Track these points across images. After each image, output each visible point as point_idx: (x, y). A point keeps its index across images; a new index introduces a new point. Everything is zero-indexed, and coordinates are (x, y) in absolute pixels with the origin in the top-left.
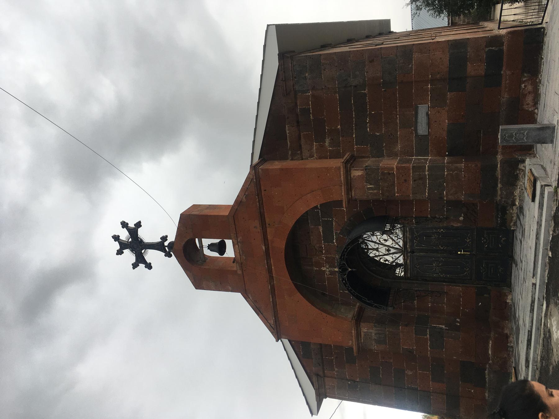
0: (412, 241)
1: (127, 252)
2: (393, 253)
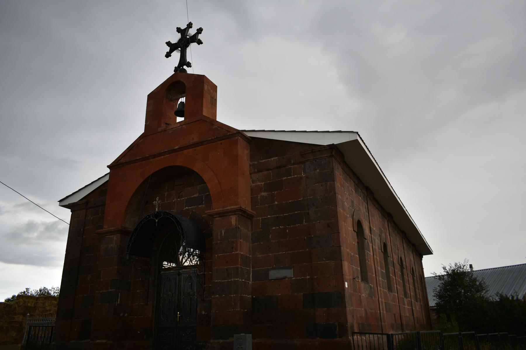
1: (179, 36)
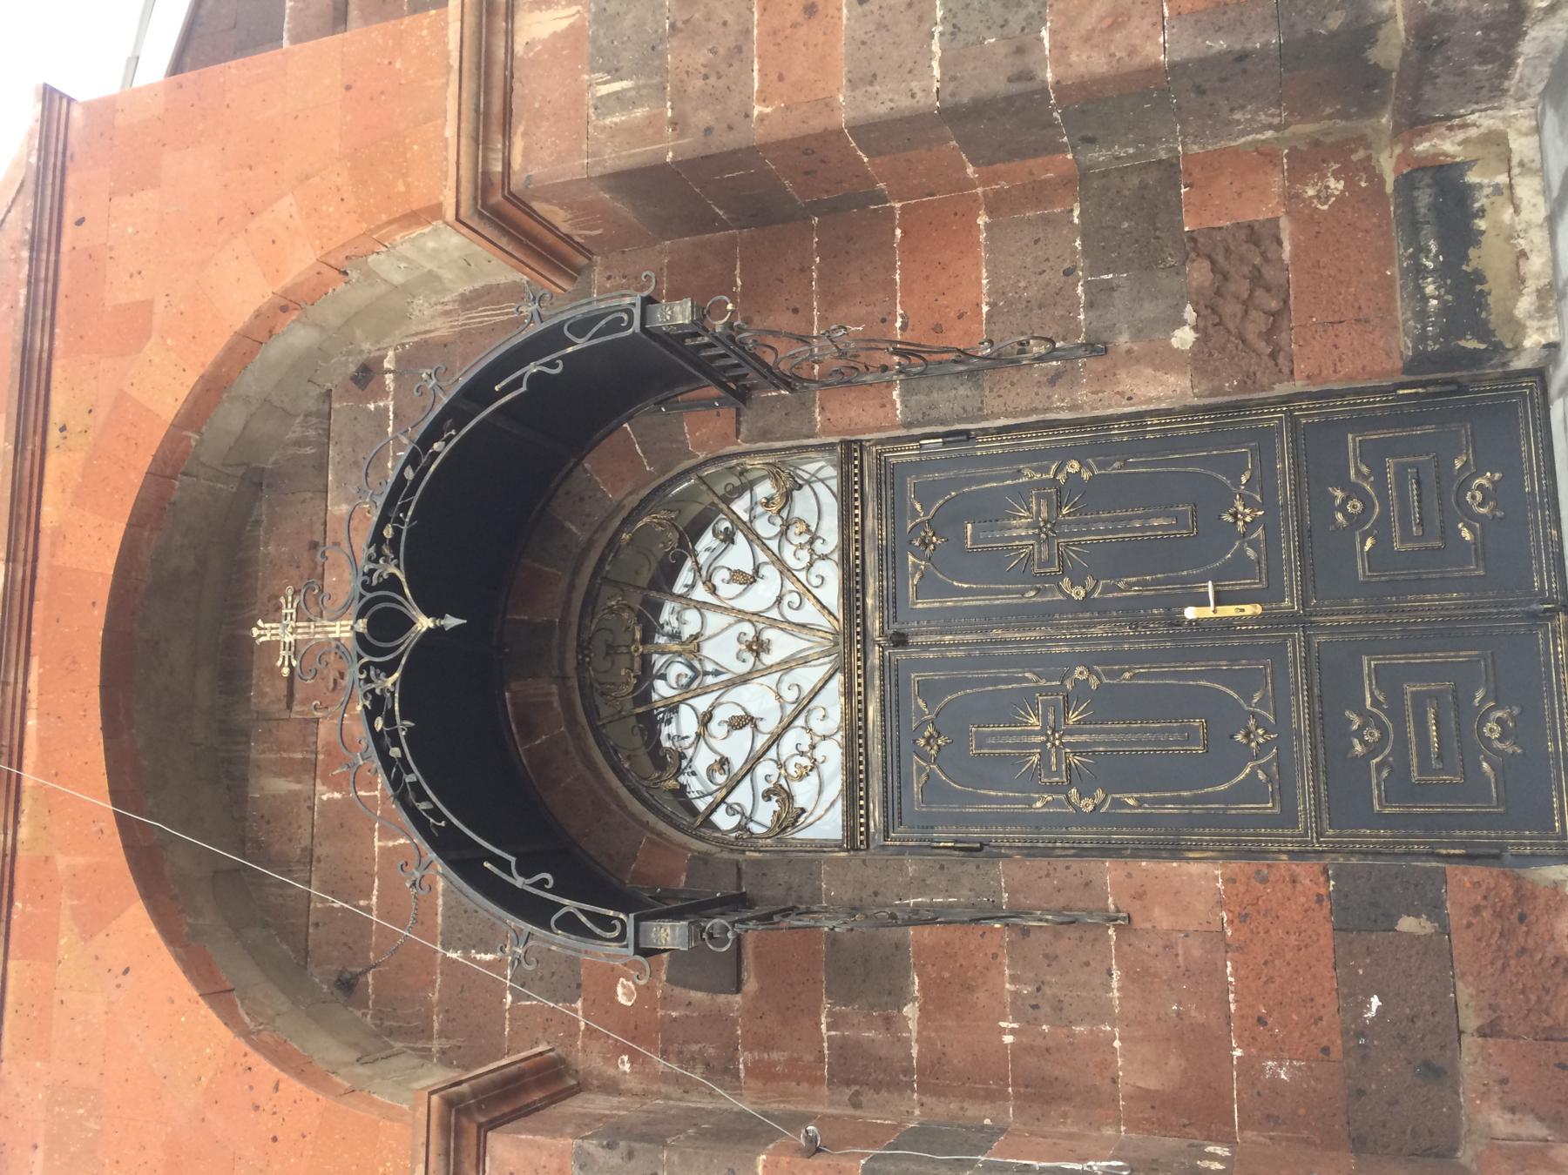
0: (891, 559)
2: (787, 665)
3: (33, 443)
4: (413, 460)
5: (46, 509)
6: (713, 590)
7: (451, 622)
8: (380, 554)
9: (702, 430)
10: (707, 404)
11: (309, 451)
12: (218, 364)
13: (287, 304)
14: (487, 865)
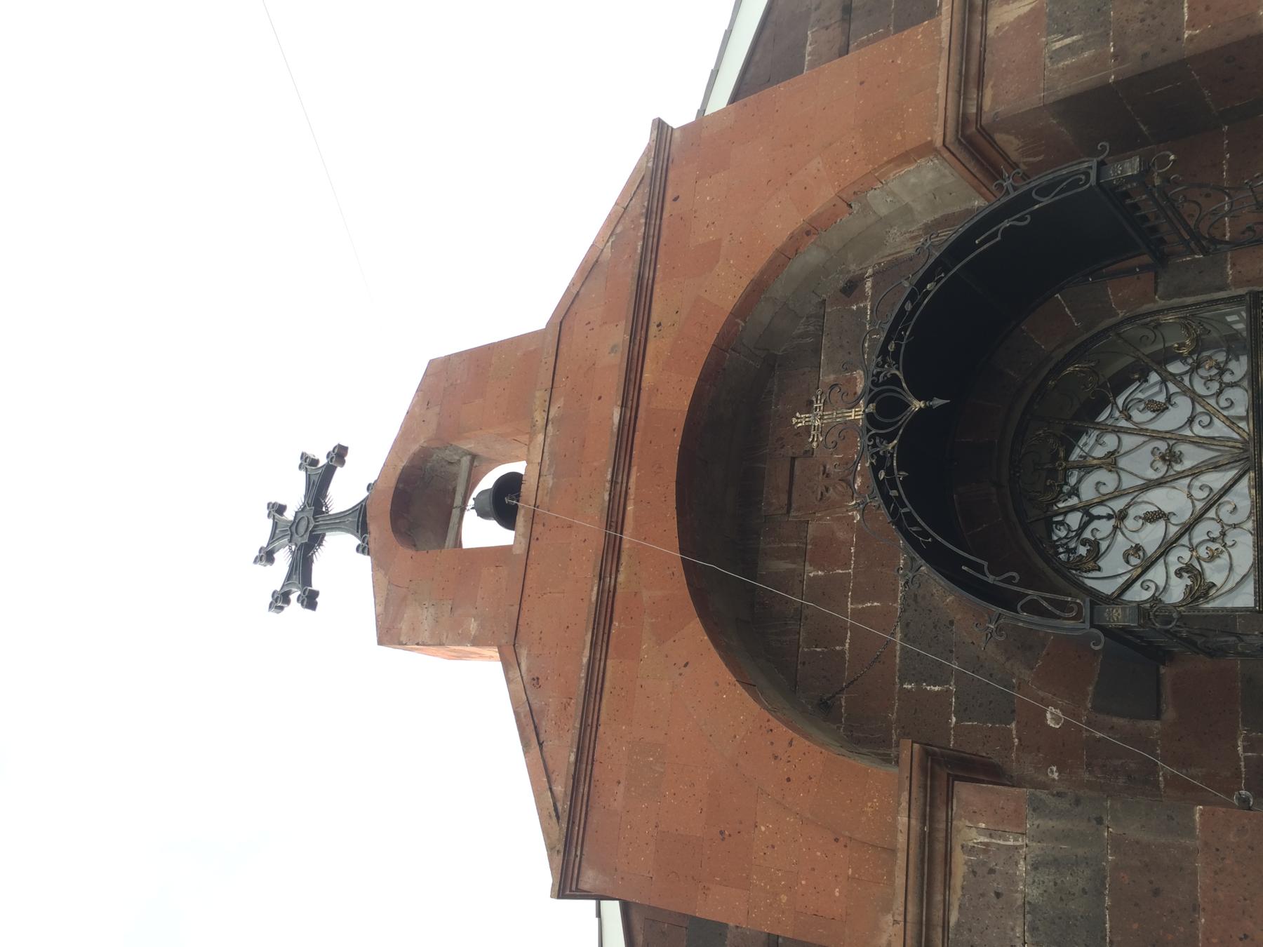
2: (1195, 473)
3: (640, 335)
4: (911, 296)
5: (646, 375)
6: (1129, 418)
7: (938, 402)
8: (884, 362)
9: (1123, 295)
10: (1130, 272)
11: (809, 340)
12: (762, 273)
13: (810, 230)
14: (964, 568)
